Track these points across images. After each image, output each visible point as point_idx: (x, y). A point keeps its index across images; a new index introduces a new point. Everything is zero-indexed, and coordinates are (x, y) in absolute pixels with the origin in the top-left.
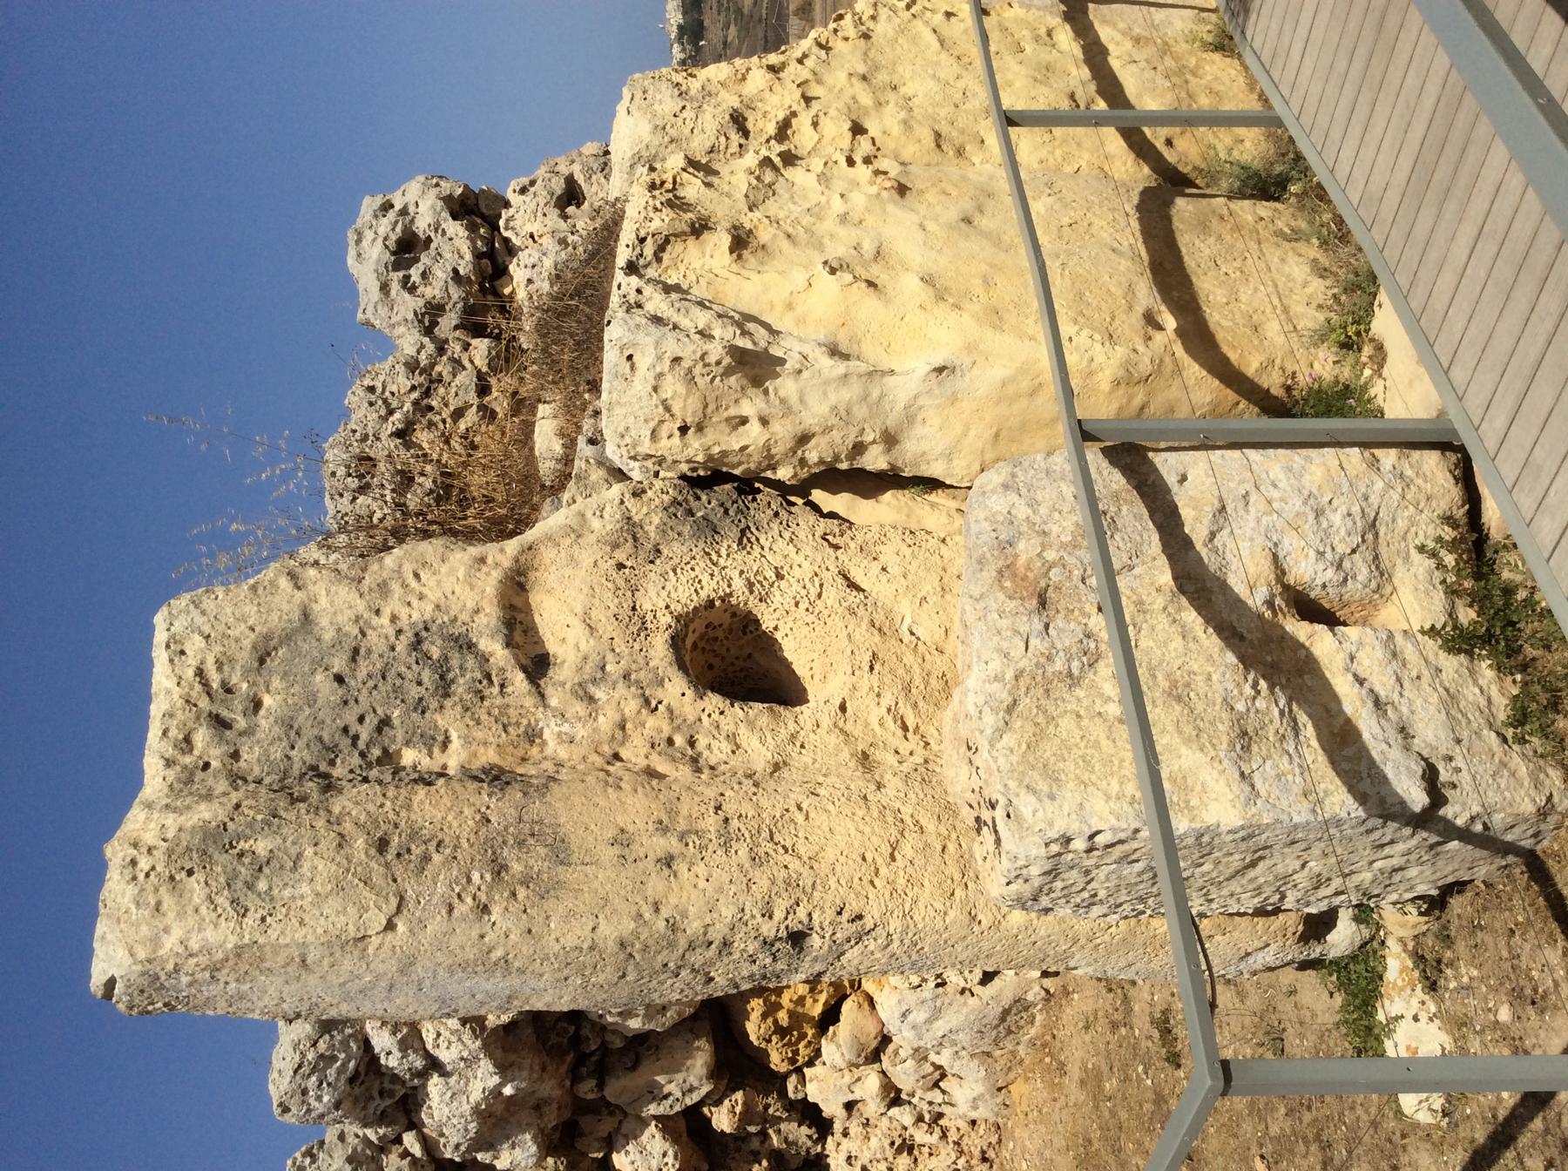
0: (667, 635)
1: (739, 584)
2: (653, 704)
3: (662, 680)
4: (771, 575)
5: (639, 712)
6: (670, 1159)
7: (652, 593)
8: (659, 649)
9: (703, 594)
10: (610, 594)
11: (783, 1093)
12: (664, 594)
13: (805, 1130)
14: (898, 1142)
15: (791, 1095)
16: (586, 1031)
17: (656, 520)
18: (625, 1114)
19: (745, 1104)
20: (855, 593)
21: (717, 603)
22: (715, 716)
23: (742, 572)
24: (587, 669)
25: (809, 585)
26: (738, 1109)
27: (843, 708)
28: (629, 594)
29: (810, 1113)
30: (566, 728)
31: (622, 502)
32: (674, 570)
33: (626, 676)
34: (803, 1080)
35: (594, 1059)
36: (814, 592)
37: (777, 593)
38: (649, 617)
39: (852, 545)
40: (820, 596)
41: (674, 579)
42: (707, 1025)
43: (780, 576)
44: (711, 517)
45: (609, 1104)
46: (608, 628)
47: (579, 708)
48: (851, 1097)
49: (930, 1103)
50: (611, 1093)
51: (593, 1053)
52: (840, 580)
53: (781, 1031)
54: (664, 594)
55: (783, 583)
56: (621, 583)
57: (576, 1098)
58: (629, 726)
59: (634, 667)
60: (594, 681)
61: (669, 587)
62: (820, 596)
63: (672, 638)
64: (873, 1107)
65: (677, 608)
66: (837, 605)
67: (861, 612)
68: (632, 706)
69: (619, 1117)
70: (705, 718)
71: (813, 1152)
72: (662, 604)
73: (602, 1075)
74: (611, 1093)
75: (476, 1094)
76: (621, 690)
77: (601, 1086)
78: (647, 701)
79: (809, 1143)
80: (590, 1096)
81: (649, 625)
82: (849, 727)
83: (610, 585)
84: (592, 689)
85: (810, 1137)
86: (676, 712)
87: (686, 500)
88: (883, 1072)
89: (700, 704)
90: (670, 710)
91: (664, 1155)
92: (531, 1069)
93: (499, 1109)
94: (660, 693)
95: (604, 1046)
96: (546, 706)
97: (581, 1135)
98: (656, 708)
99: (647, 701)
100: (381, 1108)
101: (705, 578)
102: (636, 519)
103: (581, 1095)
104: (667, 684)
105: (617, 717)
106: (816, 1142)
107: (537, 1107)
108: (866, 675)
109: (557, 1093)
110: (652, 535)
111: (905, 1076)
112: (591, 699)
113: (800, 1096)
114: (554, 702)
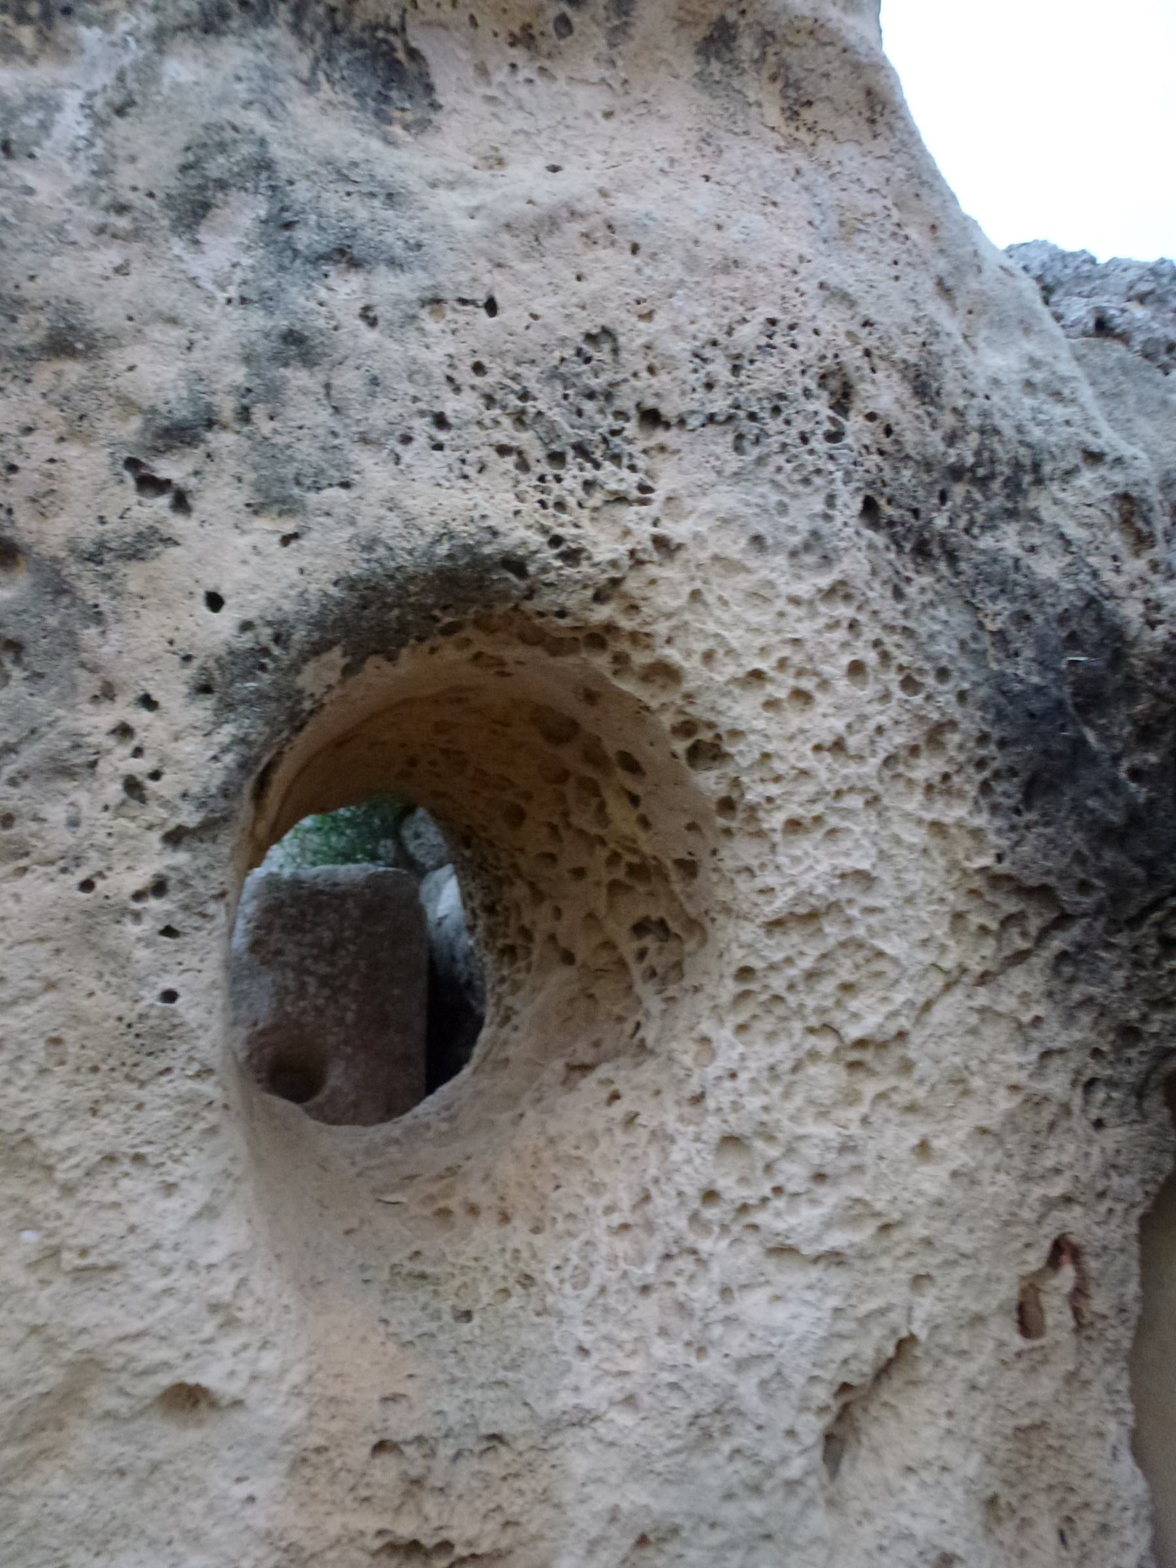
0: (521, 536)
1: (808, 868)
2: (166, 468)
3: (287, 507)
4: (868, 1017)
5: (128, 405)
7: (726, 499)
8: (445, 498)
9: (744, 710)
10: (708, 327)
12: (735, 546)
17: (1047, 567)
20: (812, 1427)
21: (710, 782)
22: (120, 761)
23: (865, 879)
24: (334, 202)
25: (831, 1198)
27: (188, 1399)
28: (719, 404)
30: (71, 123)
31: (1094, 457)
32: (839, 591)
33: (297, 345)
36: (800, 1221)
37: (781, 1051)
38: (613, 478)
39: (1046, 1386)
40: (782, 1251)
41: (803, 589)
43: (860, 1055)
44: (1088, 777)
46: (545, 304)
47: (151, 157)
52: (872, 1346)
54: (735, 546)
55: (826, 1078)
56: (766, 376)
58: (73, 371)
59: (349, 380)
60: (282, 222)
61: (773, 568)
62: (782, 1251)
63: (515, 564)
65: (666, 590)
66: (738, 1344)
67: (715, 1471)
68: (155, 373)
70: (122, 711)
72: (676, 531)
76: (231, 329)
78: (178, 435)
81: (573, 474)
82: (88, 1441)
83: (749, 335)
84: (245, 212)
86: (134, 576)
87: (1130, 691)
89: (172, 687)
90: (144, 545)
94: (220, 496)
96: (160, 38)
98: (150, 484)
99: (178, 435)
101: (824, 720)
102: (1039, 500)
104: (267, 527)
105: (105, 315)
108: (368, 1522)
110: (986, 542)
112: (193, 210)
114: (181, 68)
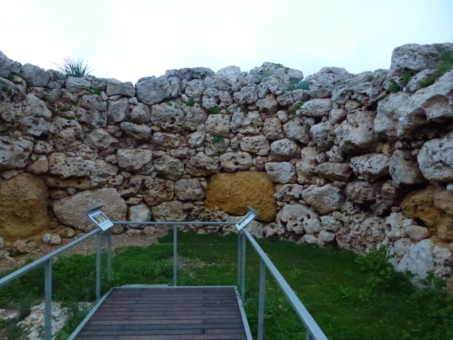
6: (375, 171)
11: (393, 205)
13: (381, 211)
14: (377, 239)
15: (393, 208)
16: (419, 143)
18: (390, 157)
19: (391, 193)
26: (389, 191)
29: (386, 213)
34: (398, 211)
35: (409, 147)
42: (419, 182)
45: (393, 152)
48: (392, 226)
49: (389, 251)
50: (397, 151)
51: (411, 146)
53: (416, 206)
57: (395, 141)
64: (389, 234)
69: (389, 155)
71: (375, 212)
73: (403, 149)
74: (397, 151)
75: (400, 109)
77: (400, 149)
79: (377, 212)
80: (396, 146)
85: (379, 212)
88: (400, 238)
91: (376, 169)
92: (408, 125)
93: (395, 116)
95: (413, 149)
97: (383, 144)
100: (396, 81)
103: (397, 143)
106: (378, 214)
107: (394, 129)
109: (398, 134)
111: (399, 244)
113: (392, 211)
